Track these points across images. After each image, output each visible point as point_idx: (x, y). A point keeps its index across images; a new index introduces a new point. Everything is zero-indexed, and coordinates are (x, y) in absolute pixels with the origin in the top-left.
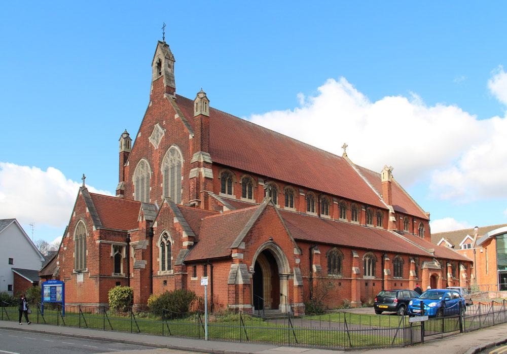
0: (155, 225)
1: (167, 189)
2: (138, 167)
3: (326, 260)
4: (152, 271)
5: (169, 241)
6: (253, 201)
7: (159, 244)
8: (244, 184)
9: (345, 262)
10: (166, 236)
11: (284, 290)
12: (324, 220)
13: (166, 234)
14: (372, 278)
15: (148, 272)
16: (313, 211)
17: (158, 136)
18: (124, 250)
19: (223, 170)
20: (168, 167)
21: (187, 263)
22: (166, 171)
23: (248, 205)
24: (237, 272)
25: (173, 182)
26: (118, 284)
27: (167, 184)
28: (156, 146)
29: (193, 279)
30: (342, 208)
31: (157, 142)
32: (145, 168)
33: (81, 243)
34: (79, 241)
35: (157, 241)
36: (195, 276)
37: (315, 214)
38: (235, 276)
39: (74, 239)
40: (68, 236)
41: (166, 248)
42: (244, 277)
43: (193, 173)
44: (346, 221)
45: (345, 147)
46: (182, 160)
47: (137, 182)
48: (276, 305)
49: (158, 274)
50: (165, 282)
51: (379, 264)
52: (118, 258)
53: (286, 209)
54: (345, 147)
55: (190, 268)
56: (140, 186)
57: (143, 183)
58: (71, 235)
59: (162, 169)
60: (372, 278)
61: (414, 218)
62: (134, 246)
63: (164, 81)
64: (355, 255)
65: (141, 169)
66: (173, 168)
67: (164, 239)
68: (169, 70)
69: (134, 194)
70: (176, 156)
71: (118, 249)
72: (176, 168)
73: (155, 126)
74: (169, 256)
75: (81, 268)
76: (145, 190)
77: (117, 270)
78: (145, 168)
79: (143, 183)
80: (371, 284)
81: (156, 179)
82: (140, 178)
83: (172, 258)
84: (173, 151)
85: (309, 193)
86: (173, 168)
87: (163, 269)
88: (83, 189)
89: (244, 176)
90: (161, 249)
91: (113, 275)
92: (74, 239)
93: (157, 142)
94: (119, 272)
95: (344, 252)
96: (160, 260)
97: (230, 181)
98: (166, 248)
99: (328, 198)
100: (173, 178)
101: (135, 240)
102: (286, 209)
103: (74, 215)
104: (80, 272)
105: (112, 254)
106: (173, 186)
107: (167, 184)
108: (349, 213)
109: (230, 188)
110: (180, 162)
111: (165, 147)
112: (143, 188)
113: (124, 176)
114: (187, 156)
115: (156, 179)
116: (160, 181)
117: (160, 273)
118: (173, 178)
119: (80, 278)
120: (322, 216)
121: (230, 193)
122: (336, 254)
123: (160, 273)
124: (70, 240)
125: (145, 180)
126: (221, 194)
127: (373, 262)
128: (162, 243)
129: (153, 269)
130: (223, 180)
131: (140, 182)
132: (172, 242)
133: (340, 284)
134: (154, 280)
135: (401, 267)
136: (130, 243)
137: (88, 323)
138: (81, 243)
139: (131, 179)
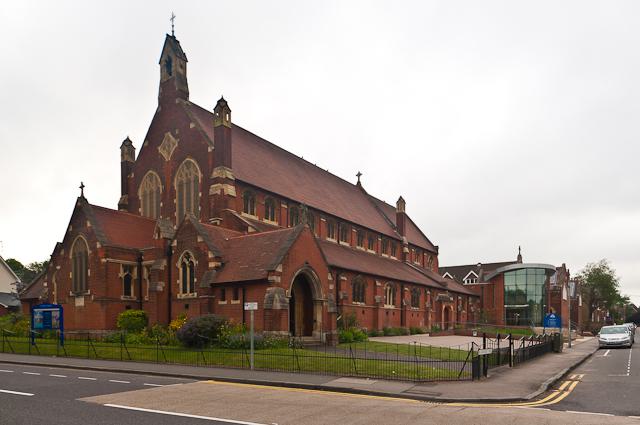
0: (175, 244)
1: (181, 206)
2: (146, 179)
3: (351, 287)
4: (170, 294)
5: (191, 262)
6: (275, 224)
7: (179, 265)
8: (267, 206)
9: (369, 290)
10: (188, 256)
11: (319, 318)
12: (343, 247)
13: (187, 253)
14: (392, 307)
15: (165, 296)
16: (333, 238)
17: (169, 146)
18: (136, 269)
19: (246, 189)
20: (182, 181)
21: (214, 286)
22: (181, 185)
23: (272, 228)
24: (279, 296)
25: (189, 198)
26: (128, 308)
27: (181, 200)
28: (168, 158)
29: (221, 303)
30: (360, 237)
31: (169, 154)
32: (154, 181)
33: (81, 261)
34: (78, 260)
35: (177, 261)
36: (236, 299)
37: (335, 241)
38: (272, 299)
39: (71, 257)
40: (62, 253)
41: (188, 269)
42: (282, 301)
43: (215, 189)
44: (363, 249)
45: (359, 175)
46: (200, 175)
47: (144, 196)
48: (308, 332)
49: (178, 297)
50: (187, 307)
51: (398, 295)
52: (128, 279)
53: (266, 221)
54: (359, 175)
55: (218, 291)
56: (148, 201)
57: (151, 198)
58: (67, 252)
59: (175, 184)
60: (392, 307)
61: (424, 250)
62: (148, 267)
63: (176, 83)
64: (378, 284)
65: (149, 182)
66: (188, 183)
67: (185, 260)
68: (181, 71)
69: (140, 210)
70: (192, 169)
71: (127, 268)
72: (192, 184)
73: (166, 135)
74: (192, 278)
75: (81, 289)
76: (155, 205)
77: (128, 293)
78: (154, 181)
79: (151, 198)
80: (391, 313)
81: (168, 194)
82: (148, 192)
83: (195, 280)
84: (188, 164)
85: (291, 205)
86: (188, 183)
87: (185, 291)
88: (82, 200)
89: (267, 196)
90: (181, 269)
91: (122, 298)
92: (71, 257)
93: (169, 154)
94: (129, 294)
95: (369, 281)
96: (180, 282)
97: (253, 202)
98: (188, 269)
99: (347, 225)
100: (188, 193)
101: (149, 259)
102: (266, 221)
103: (71, 229)
104: (79, 295)
105: (122, 274)
106: (189, 202)
107: (181, 200)
108: (366, 241)
109: (252, 207)
110: (197, 177)
111: (178, 158)
112: (151, 203)
113: (127, 186)
114: (207, 172)
115: (168, 194)
116: (173, 196)
117: (181, 295)
118: (188, 193)
119: (80, 302)
120: (341, 243)
121: (252, 214)
122: (362, 282)
123: (181, 295)
124: (66, 258)
125: (155, 195)
126: (244, 214)
127: (393, 291)
128: (184, 264)
129: (172, 291)
130: (246, 199)
131: (148, 197)
132: (196, 263)
133: (363, 312)
134: (173, 303)
135: (418, 298)
136: (144, 263)
137: (67, 351)
138: (81, 261)
139: (136, 192)
